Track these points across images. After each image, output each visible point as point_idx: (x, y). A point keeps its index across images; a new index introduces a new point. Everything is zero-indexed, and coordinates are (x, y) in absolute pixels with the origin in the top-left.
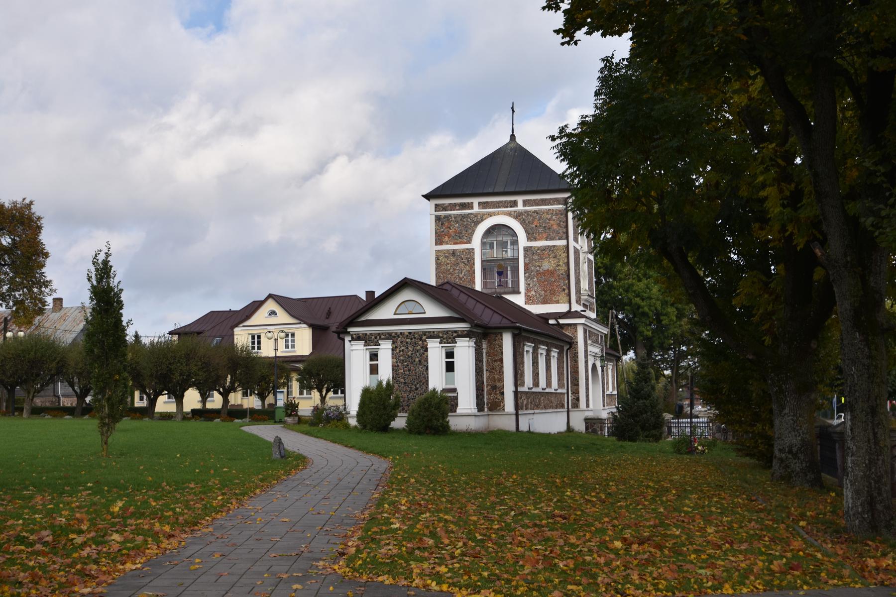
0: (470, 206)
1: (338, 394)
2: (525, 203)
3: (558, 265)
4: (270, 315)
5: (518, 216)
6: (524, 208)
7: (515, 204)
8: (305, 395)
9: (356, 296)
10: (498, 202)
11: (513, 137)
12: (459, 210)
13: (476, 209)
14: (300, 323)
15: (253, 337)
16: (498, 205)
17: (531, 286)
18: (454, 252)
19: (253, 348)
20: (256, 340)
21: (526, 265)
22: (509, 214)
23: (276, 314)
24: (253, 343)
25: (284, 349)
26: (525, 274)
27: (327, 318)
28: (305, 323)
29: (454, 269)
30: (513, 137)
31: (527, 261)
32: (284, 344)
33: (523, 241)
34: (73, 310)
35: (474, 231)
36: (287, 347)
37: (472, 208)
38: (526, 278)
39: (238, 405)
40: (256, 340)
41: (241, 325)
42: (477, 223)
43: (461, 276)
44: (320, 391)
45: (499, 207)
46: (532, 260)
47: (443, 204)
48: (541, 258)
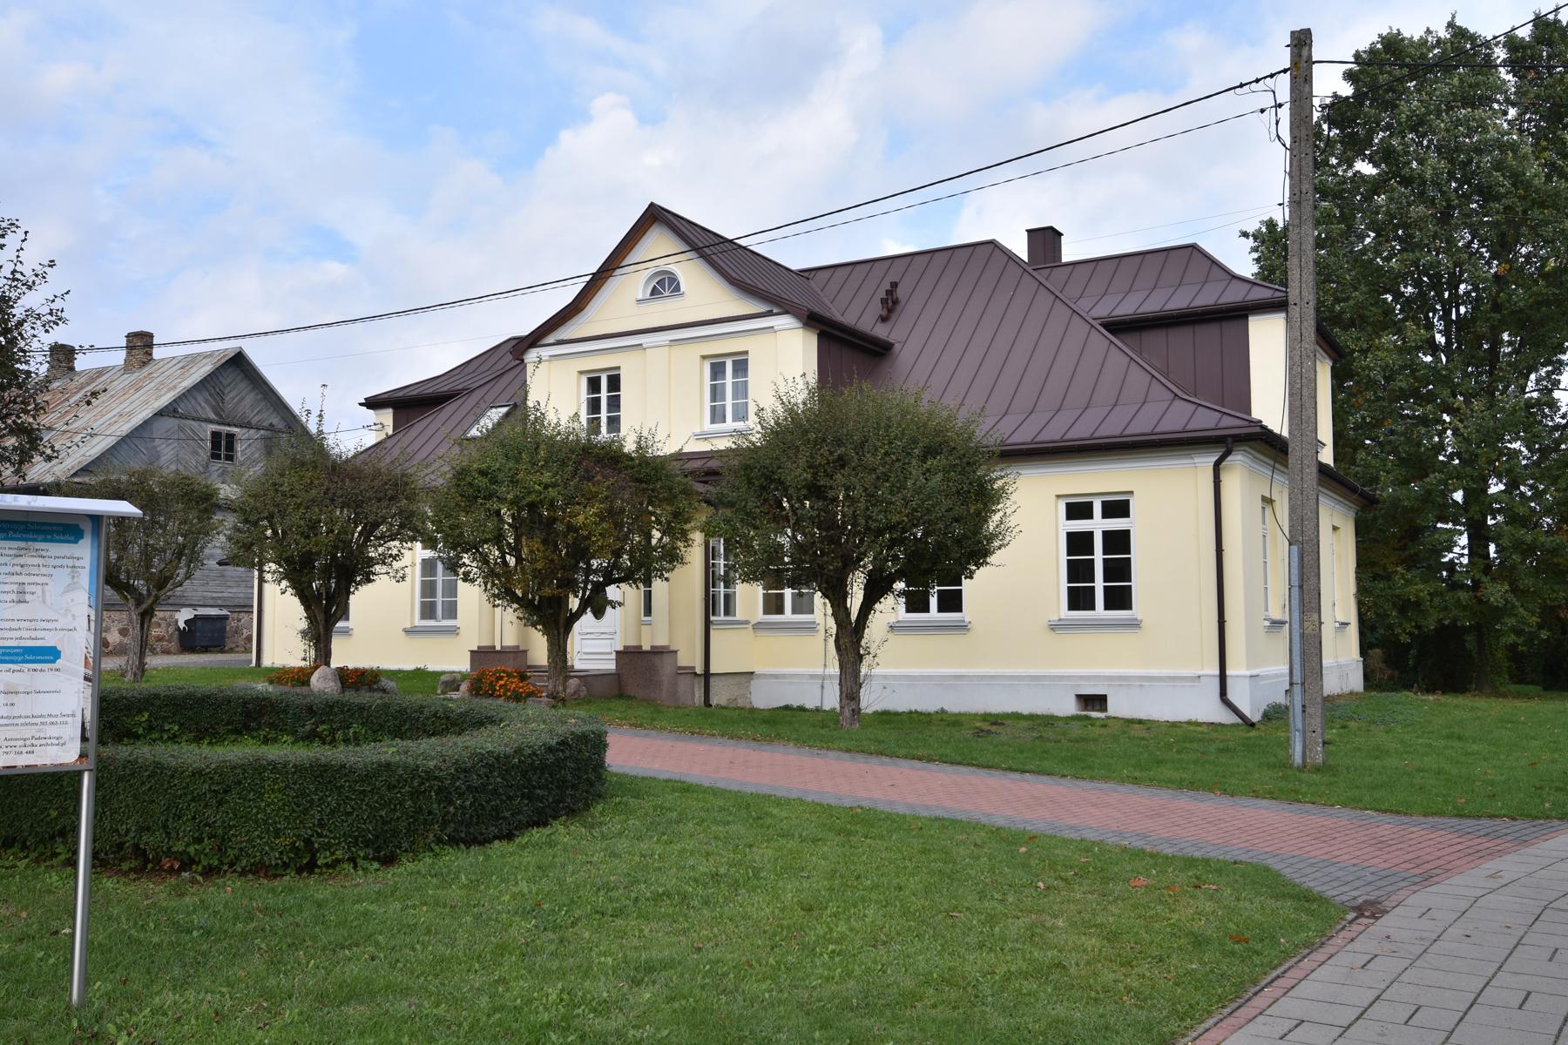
1: (926, 609)
4: (654, 292)
8: (788, 615)
9: (993, 244)
14: (769, 314)
15: (594, 384)
19: (594, 425)
20: (604, 394)
23: (677, 288)
24: (594, 406)
25: (708, 427)
27: (884, 319)
28: (786, 308)
32: (708, 404)
34: (174, 362)
36: (717, 415)
39: (505, 652)
40: (604, 394)
41: (551, 339)
44: (837, 596)
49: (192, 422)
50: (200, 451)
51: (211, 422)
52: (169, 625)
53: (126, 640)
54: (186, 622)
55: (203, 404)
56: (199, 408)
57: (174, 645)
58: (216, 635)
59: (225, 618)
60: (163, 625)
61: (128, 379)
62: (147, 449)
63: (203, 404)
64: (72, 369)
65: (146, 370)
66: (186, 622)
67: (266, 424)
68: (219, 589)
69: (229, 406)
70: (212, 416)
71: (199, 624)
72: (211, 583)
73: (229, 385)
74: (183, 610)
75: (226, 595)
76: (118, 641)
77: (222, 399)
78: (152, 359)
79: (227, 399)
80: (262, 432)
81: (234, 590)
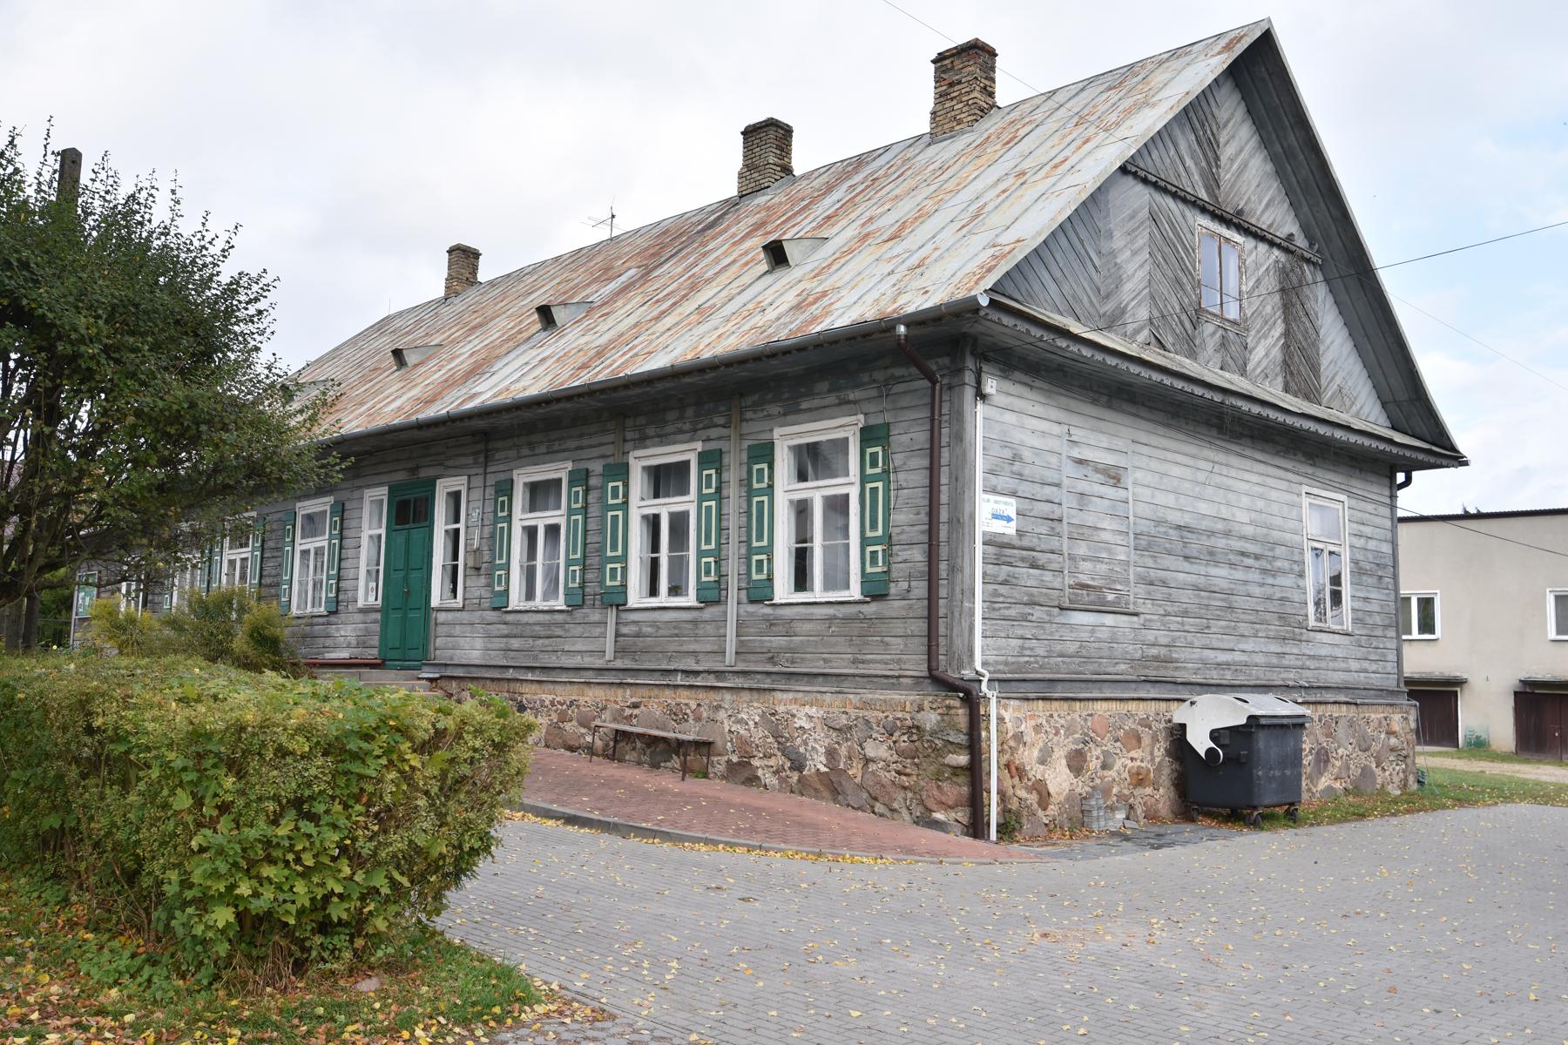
49: (1170, 201)
50: (1185, 280)
51: (1203, 210)
52: (1155, 739)
53: (1081, 787)
54: (1215, 735)
55: (1189, 162)
56: (1181, 168)
57: (1161, 796)
58: (1288, 772)
59: (1296, 726)
60: (1146, 740)
61: (949, 149)
62: (1099, 253)
63: (1189, 162)
64: (787, 170)
65: (990, 125)
66: (1215, 735)
67: (1282, 232)
68: (1228, 642)
69: (1226, 177)
70: (1203, 194)
71: (1262, 740)
72: (1217, 626)
73: (1225, 125)
74: (1205, 700)
75: (1238, 657)
76: (1066, 787)
77: (1217, 158)
78: (993, 106)
79: (1224, 159)
80: (1276, 252)
81: (1248, 646)
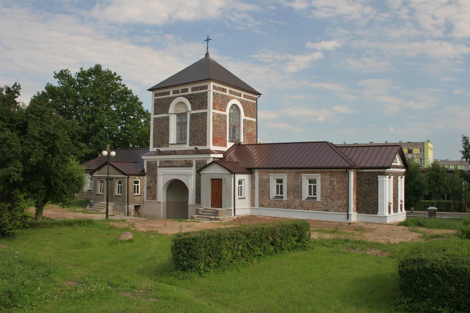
0: (224, 90)
2: (245, 96)
3: (253, 131)
5: (242, 102)
6: (244, 98)
7: (240, 95)
10: (236, 92)
11: (207, 55)
12: (222, 91)
13: (228, 93)
16: (235, 94)
17: (245, 140)
18: (219, 115)
21: (244, 128)
22: (239, 100)
26: (243, 133)
29: (220, 125)
30: (207, 55)
31: (244, 127)
33: (243, 116)
35: (227, 105)
37: (226, 92)
38: (244, 135)
42: (228, 101)
43: (222, 129)
45: (235, 95)
46: (245, 126)
47: (216, 86)
48: (248, 126)
